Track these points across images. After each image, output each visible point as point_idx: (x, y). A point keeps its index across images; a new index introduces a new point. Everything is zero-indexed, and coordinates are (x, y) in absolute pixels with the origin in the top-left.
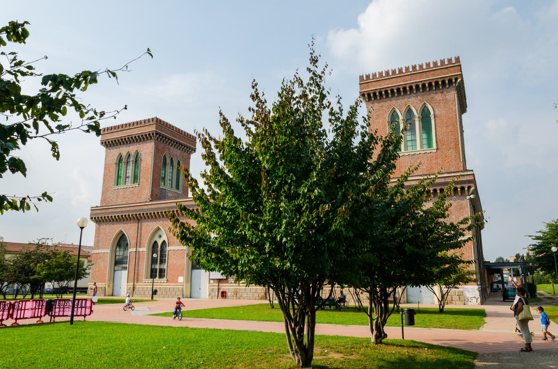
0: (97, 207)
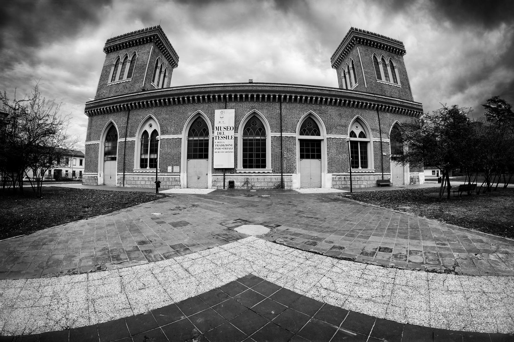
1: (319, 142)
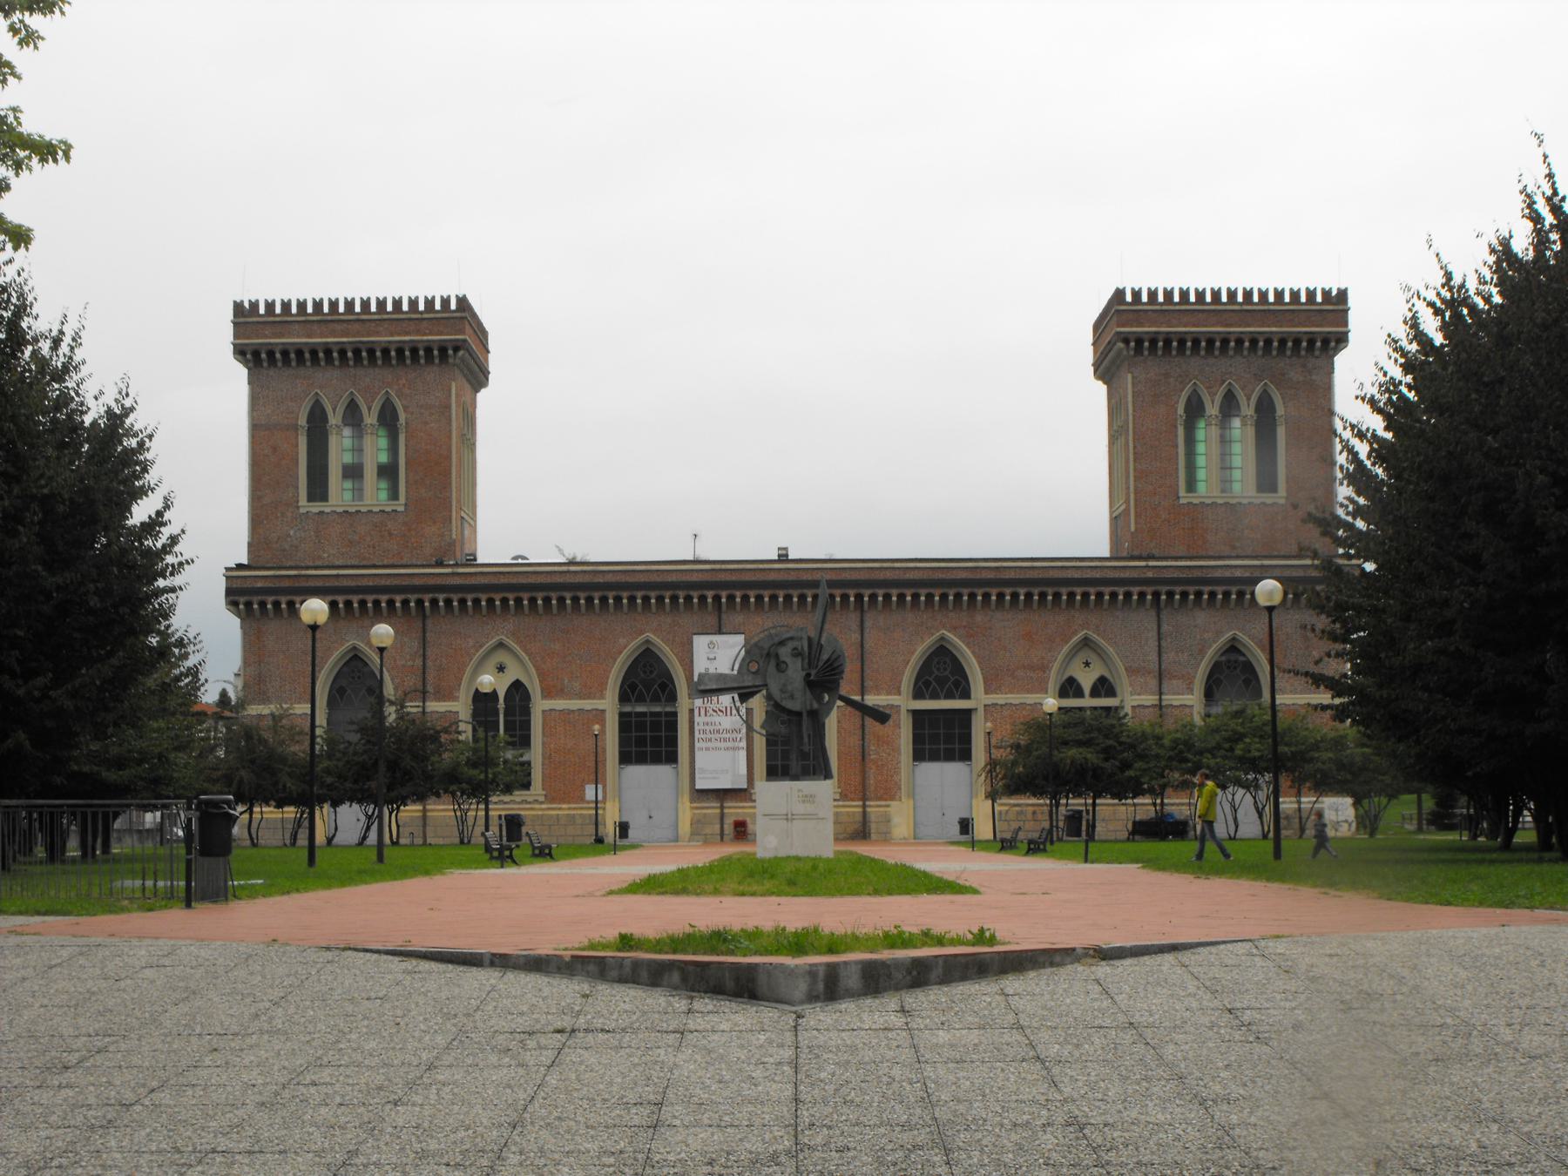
0: (240, 567)
1: (967, 714)
